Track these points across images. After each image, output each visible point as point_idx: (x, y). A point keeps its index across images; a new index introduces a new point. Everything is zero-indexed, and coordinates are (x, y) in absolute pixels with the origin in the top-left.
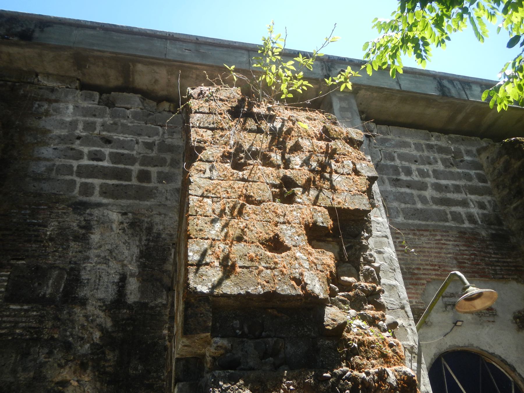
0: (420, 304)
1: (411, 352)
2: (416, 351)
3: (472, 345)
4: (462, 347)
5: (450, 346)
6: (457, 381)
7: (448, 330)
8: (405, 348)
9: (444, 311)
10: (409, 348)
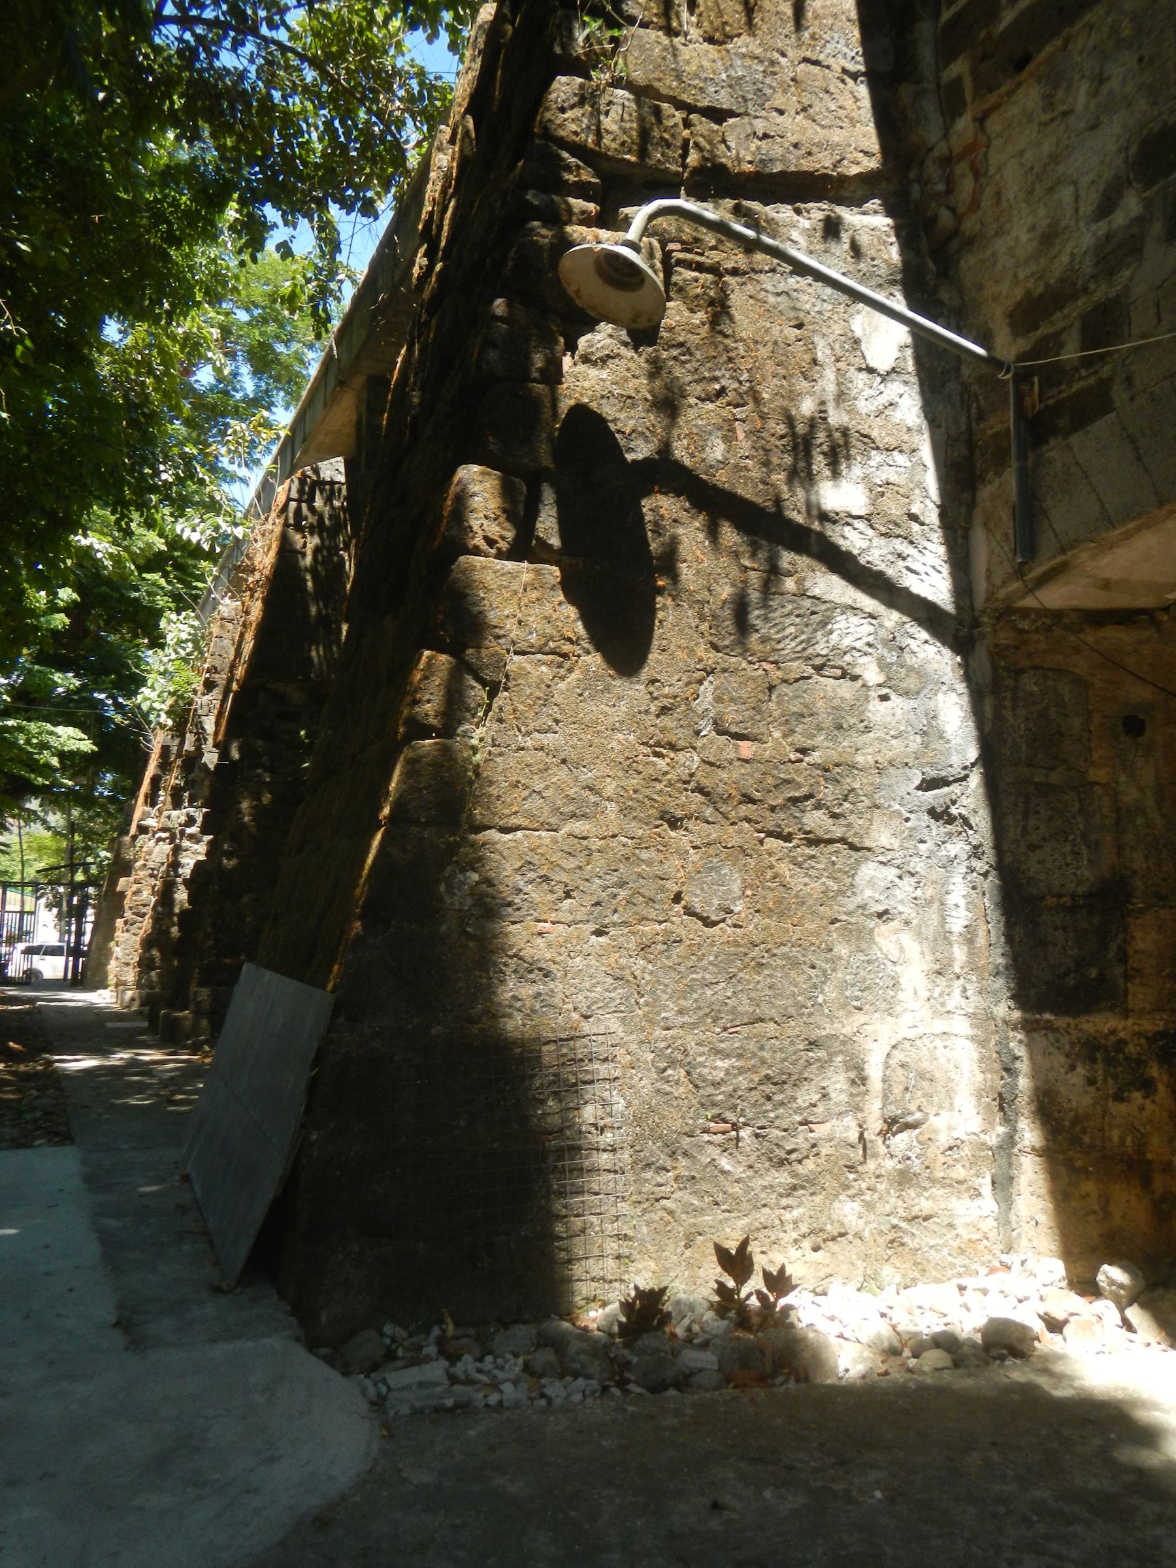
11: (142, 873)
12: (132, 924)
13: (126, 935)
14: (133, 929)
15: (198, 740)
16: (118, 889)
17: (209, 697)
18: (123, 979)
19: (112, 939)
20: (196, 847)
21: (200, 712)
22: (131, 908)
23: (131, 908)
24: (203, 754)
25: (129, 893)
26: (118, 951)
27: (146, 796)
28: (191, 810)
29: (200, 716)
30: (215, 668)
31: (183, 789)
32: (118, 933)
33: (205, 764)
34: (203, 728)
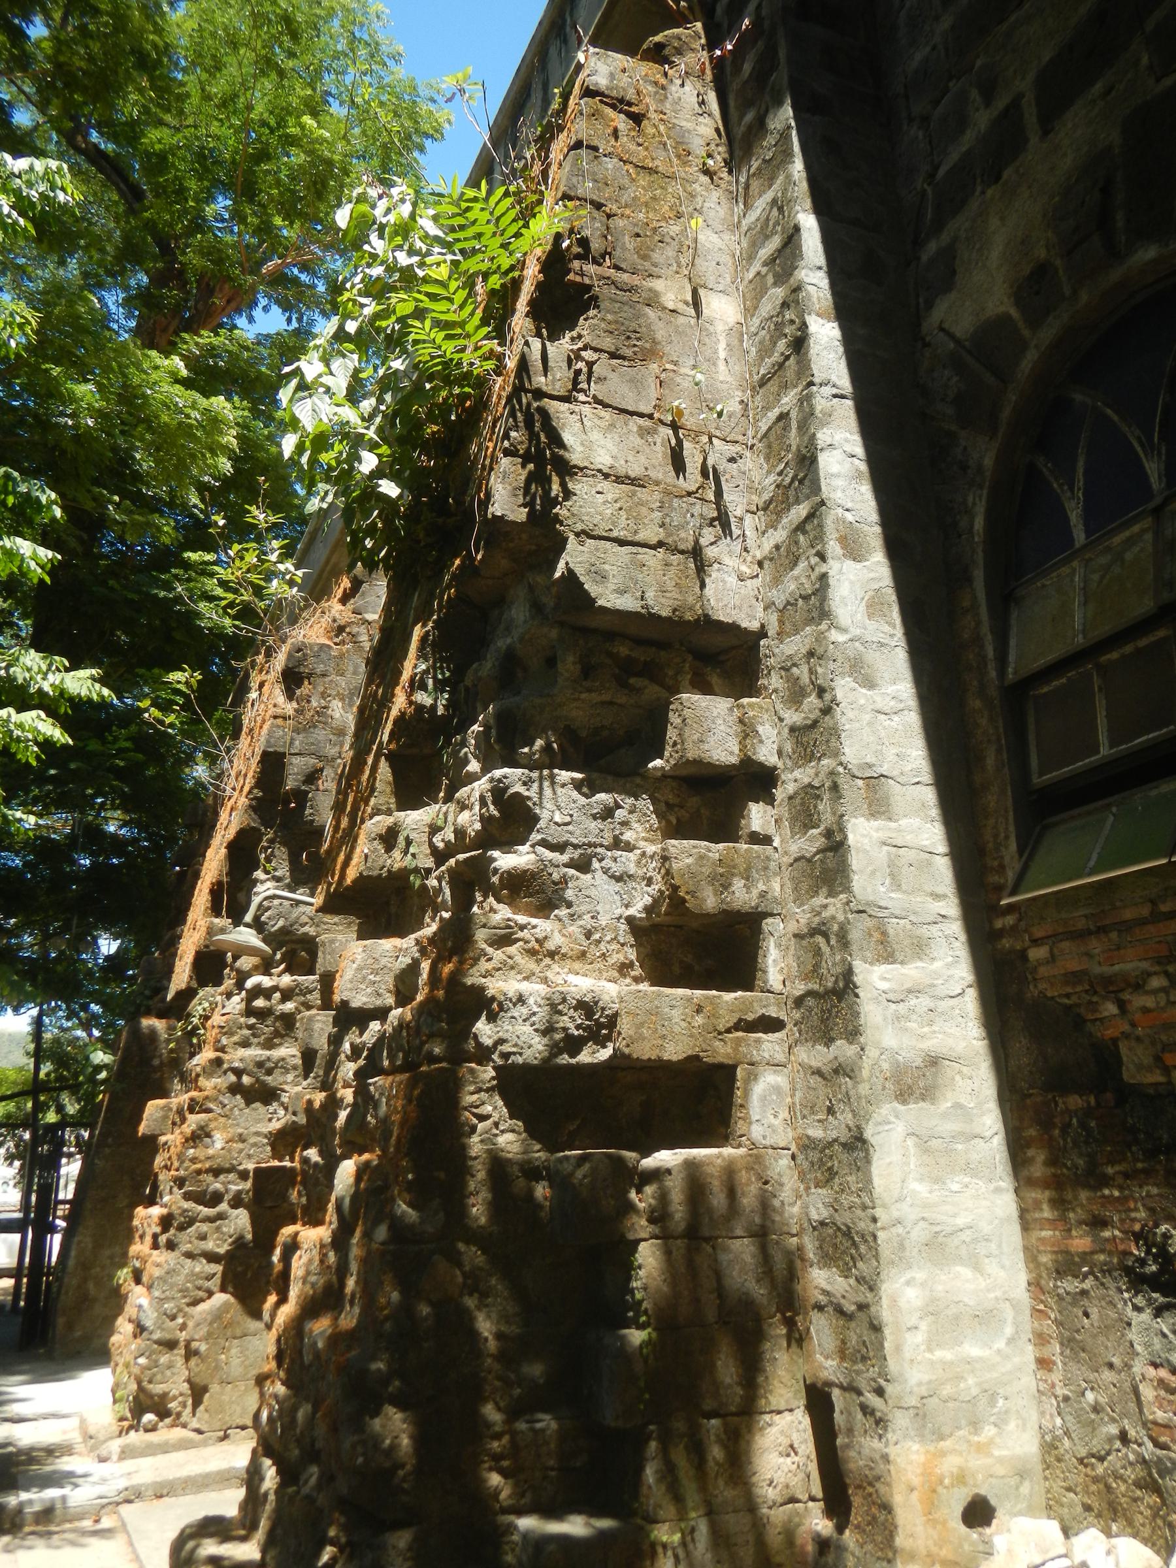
11: (209, 1084)
12: (182, 1228)
13: (160, 1256)
15: (538, 478)
16: (142, 1129)
17: (560, 348)
18: (157, 1389)
19: (123, 1259)
20: (543, 926)
21: (540, 381)
22: (180, 1182)
23: (180, 1182)
24: (559, 545)
25: (172, 1139)
26: (139, 1298)
27: (216, 892)
28: (511, 775)
29: (539, 394)
30: (584, 242)
31: (460, 715)
32: (139, 1248)
33: (571, 575)
34: (556, 440)
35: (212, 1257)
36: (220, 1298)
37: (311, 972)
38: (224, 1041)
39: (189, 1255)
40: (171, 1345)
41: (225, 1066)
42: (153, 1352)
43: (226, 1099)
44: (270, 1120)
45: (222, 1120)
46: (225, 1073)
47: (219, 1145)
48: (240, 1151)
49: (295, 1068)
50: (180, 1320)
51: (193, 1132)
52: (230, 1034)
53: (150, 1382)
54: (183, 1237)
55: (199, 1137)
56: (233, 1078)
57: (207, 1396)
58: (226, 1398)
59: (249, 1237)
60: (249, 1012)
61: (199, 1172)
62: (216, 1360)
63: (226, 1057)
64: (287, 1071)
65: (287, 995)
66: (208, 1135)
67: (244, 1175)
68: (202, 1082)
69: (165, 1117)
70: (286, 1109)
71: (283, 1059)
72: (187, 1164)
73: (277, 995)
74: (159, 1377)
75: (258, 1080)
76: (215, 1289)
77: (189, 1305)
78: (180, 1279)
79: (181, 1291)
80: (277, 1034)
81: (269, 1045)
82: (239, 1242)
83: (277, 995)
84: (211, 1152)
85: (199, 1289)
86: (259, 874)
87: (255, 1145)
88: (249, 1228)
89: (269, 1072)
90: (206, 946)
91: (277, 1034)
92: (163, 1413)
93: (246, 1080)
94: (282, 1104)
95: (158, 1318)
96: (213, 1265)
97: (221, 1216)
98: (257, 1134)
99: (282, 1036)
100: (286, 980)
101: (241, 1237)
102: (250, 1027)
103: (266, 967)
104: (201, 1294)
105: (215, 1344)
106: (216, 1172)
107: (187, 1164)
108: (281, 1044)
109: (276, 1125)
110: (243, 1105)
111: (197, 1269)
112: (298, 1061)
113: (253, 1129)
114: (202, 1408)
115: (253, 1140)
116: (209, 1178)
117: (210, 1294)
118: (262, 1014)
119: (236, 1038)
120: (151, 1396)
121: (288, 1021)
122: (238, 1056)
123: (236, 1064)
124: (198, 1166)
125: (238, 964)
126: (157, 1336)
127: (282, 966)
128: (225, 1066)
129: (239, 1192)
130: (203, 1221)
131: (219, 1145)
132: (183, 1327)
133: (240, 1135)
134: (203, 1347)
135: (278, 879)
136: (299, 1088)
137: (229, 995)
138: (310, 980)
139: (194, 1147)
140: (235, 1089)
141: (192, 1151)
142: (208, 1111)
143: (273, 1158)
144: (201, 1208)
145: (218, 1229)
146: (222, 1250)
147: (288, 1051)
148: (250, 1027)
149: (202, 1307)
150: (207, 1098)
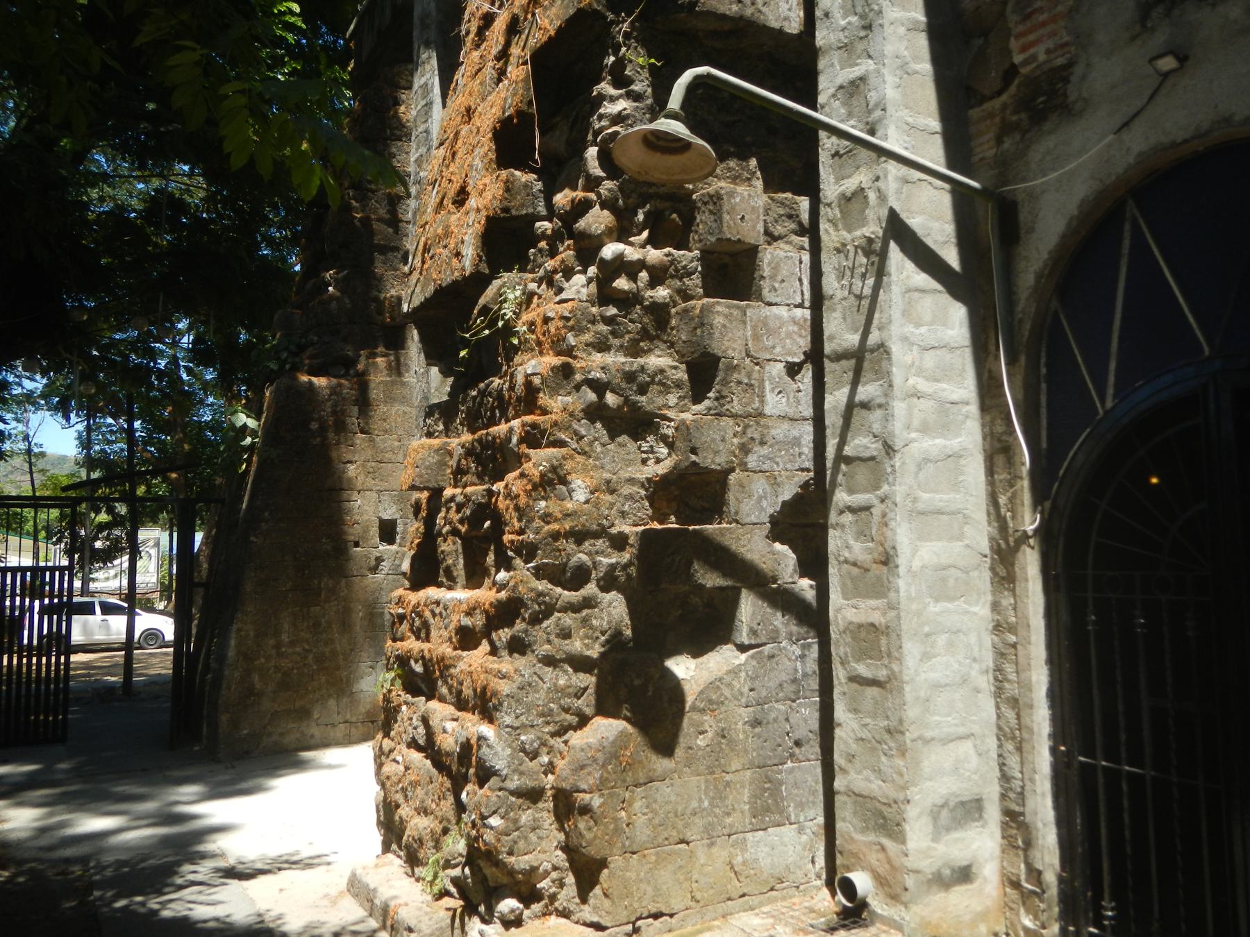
0: (1060, 52)
1: (867, 254)
2: (877, 246)
3: (1227, 120)
4: (1186, 141)
5: (1140, 154)
6: (1162, 263)
7: (1138, 104)
8: (856, 247)
9: (1134, 38)
10: (863, 242)
11: (557, 404)
12: (536, 620)
14: (544, 638)
35: (580, 664)
36: (606, 729)
37: (682, 245)
38: (571, 339)
39: (549, 661)
40: (533, 795)
41: (578, 377)
42: (511, 807)
43: (582, 427)
44: (644, 462)
45: (579, 458)
46: (577, 388)
47: (580, 496)
48: (612, 505)
49: (678, 385)
50: (545, 759)
51: (542, 475)
52: (578, 330)
53: (510, 853)
54: (538, 633)
55: (551, 483)
56: (592, 396)
57: (606, 871)
58: (631, 875)
59: (628, 633)
60: (605, 295)
61: (556, 536)
62: (616, 820)
63: (577, 364)
64: (666, 388)
65: (658, 275)
66: (564, 481)
67: (619, 542)
68: (543, 399)
69: (442, 464)
70: (671, 446)
71: (662, 371)
72: (537, 523)
73: (644, 275)
74: (521, 844)
75: (627, 400)
76: (589, 711)
77: (553, 735)
78: (540, 697)
79: (542, 715)
80: (645, 334)
81: (634, 350)
82: (615, 641)
83: (644, 275)
84: (570, 505)
85: (566, 710)
86: (605, 87)
87: (630, 497)
88: (627, 620)
89: (643, 390)
90: (506, 210)
91: (645, 334)
92: (529, 896)
93: (611, 399)
94: (664, 439)
95: (512, 756)
96: (581, 675)
97: (588, 603)
98: (631, 481)
99: (651, 339)
100: (654, 255)
101: (618, 634)
102: (609, 321)
103: (622, 233)
104: (574, 720)
105: (611, 795)
106: (580, 536)
107: (537, 523)
108: (650, 351)
109: (662, 469)
110: (606, 439)
111: (562, 682)
112: (681, 374)
113: (625, 475)
114: (597, 890)
115: (626, 490)
116: (571, 546)
117: (583, 721)
118: (627, 301)
119: (587, 337)
120: (511, 872)
121: (659, 312)
122: (596, 363)
123: (597, 374)
124: (555, 526)
125: (581, 224)
126: (513, 784)
127: (645, 234)
128: (578, 377)
129: (613, 567)
130: (564, 610)
131: (580, 496)
132: (550, 768)
133: (608, 482)
134: (596, 801)
135: (636, 97)
136: (687, 416)
137: (568, 273)
138: (688, 257)
139: (545, 498)
140: (595, 413)
141: (543, 504)
142: (560, 444)
143: (652, 519)
144: (559, 590)
145: (585, 621)
146: (595, 652)
147: (657, 360)
148: (609, 321)
149: (577, 739)
150: (555, 424)
